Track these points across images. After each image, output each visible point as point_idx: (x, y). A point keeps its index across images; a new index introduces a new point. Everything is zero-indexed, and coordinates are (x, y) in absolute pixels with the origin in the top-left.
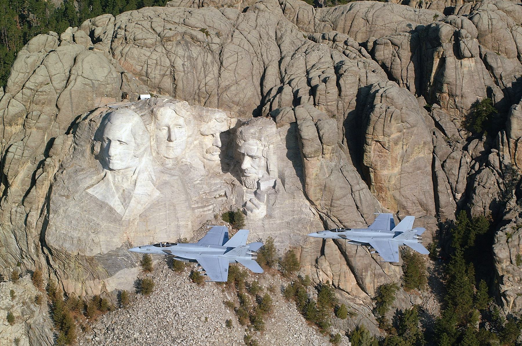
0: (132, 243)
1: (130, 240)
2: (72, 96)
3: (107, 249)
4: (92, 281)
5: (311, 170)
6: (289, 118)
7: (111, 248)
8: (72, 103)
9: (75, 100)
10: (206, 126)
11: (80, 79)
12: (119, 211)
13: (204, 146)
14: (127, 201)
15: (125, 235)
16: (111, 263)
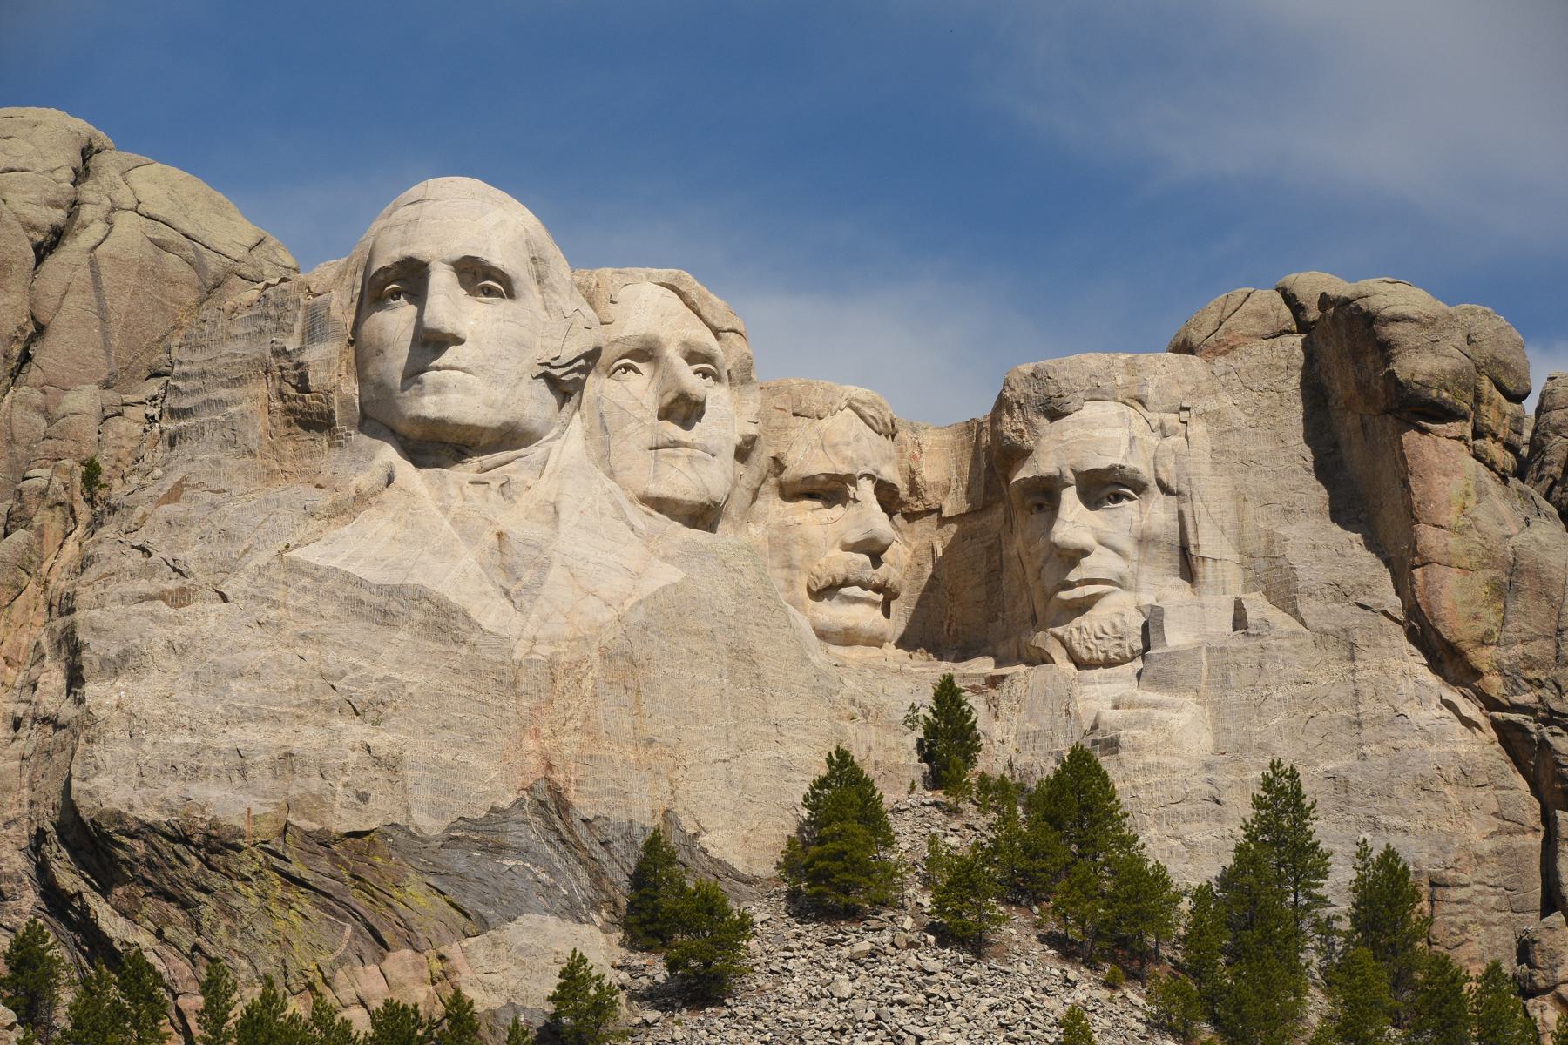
0: (572, 795)
1: (559, 777)
2: (105, 282)
3: (436, 811)
4: (373, 969)
5: (1438, 478)
6: (1261, 316)
7: (459, 807)
8: (103, 314)
9: (120, 303)
10: (813, 438)
11: (127, 224)
12: (489, 622)
13: (798, 553)
14: (527, 576)
15: (530, 744)
16: (475, 865)
